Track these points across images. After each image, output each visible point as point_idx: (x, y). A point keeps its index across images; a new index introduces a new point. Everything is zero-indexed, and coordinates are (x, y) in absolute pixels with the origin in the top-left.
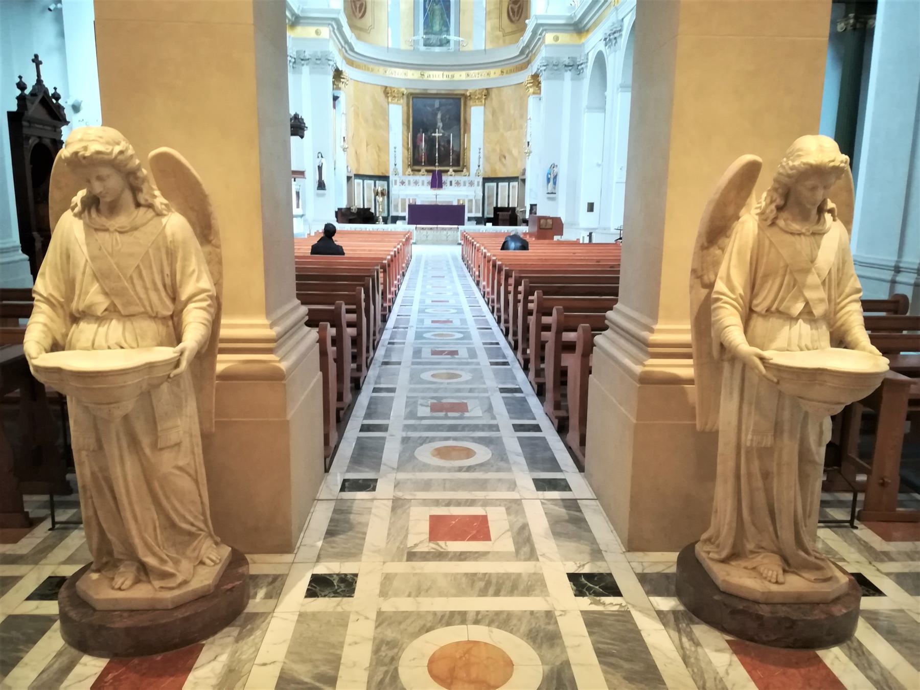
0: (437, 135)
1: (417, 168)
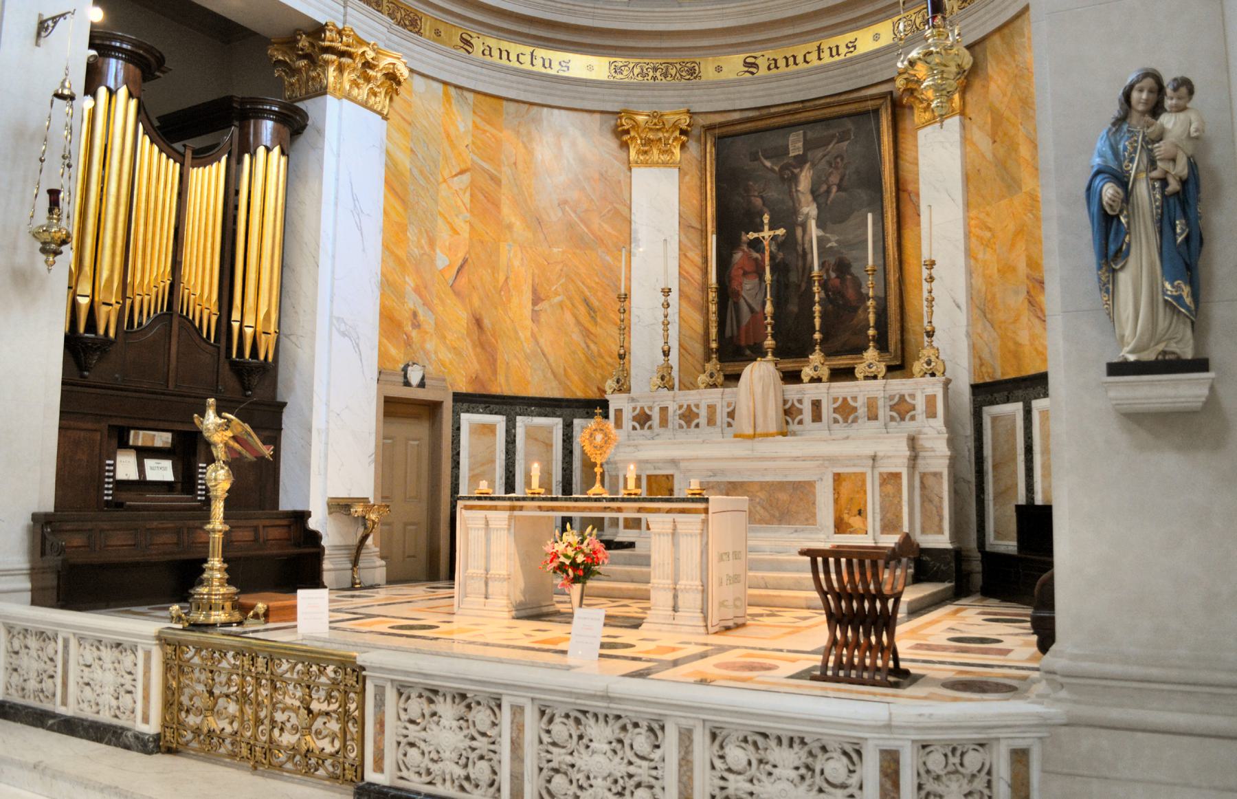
0: (766, 234)
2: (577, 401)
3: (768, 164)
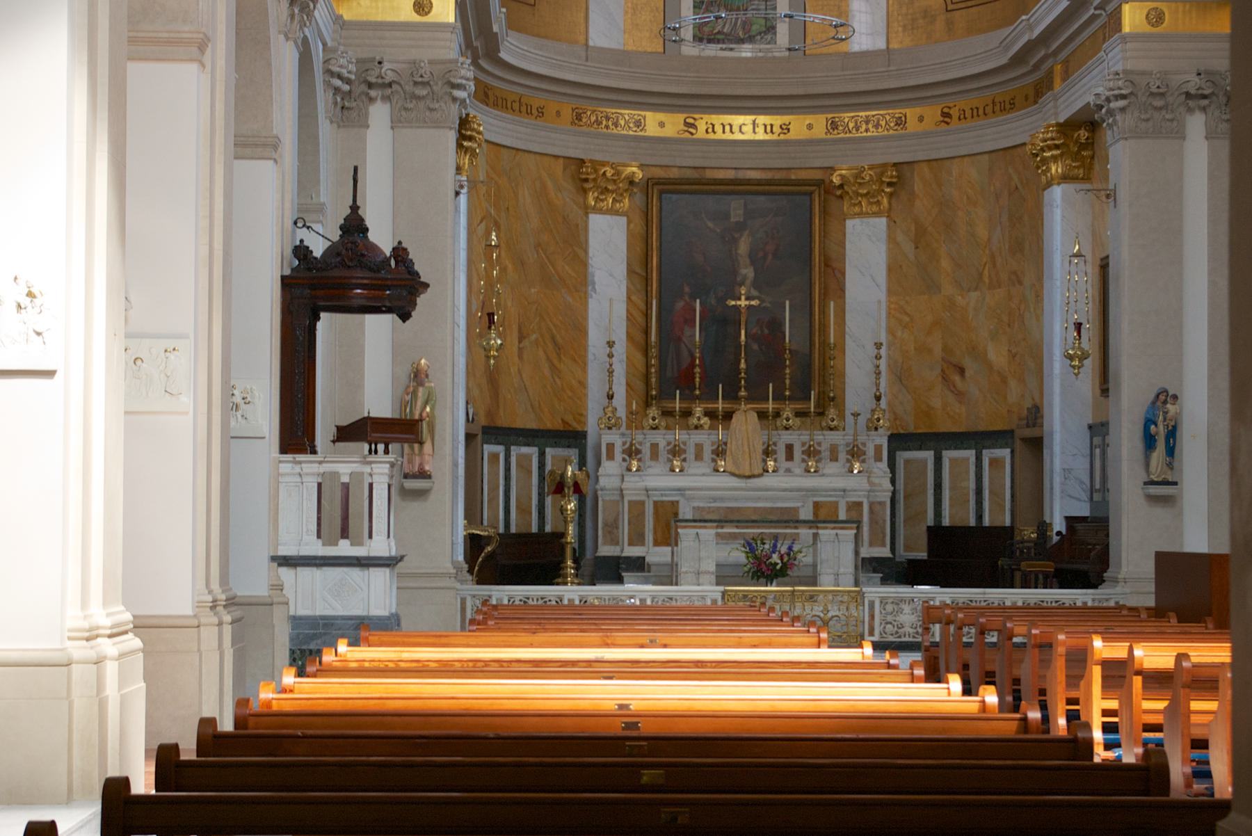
3: (710, 224)
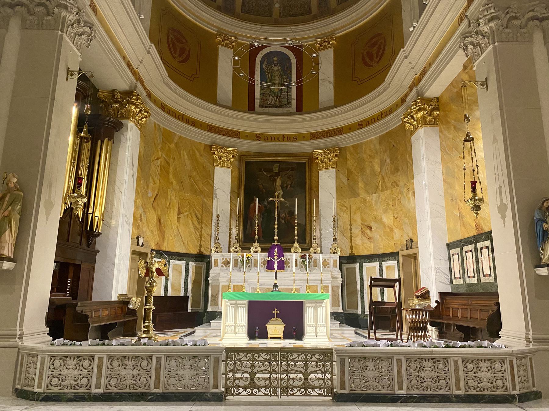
1: (247, 245)
2: (192, 254)
3: (265, 174)
